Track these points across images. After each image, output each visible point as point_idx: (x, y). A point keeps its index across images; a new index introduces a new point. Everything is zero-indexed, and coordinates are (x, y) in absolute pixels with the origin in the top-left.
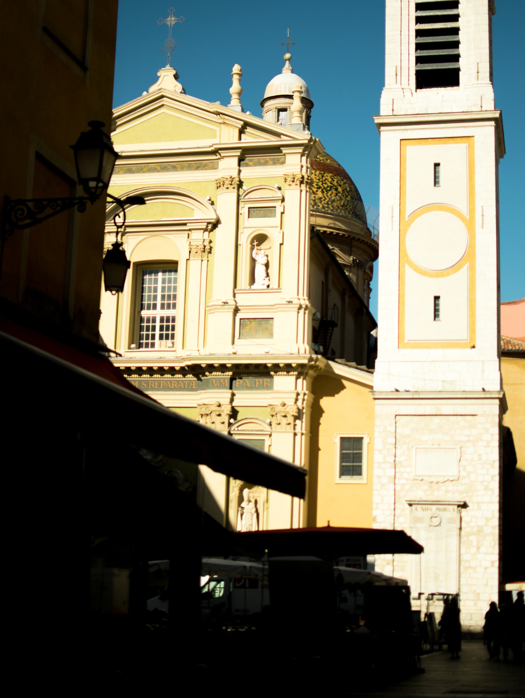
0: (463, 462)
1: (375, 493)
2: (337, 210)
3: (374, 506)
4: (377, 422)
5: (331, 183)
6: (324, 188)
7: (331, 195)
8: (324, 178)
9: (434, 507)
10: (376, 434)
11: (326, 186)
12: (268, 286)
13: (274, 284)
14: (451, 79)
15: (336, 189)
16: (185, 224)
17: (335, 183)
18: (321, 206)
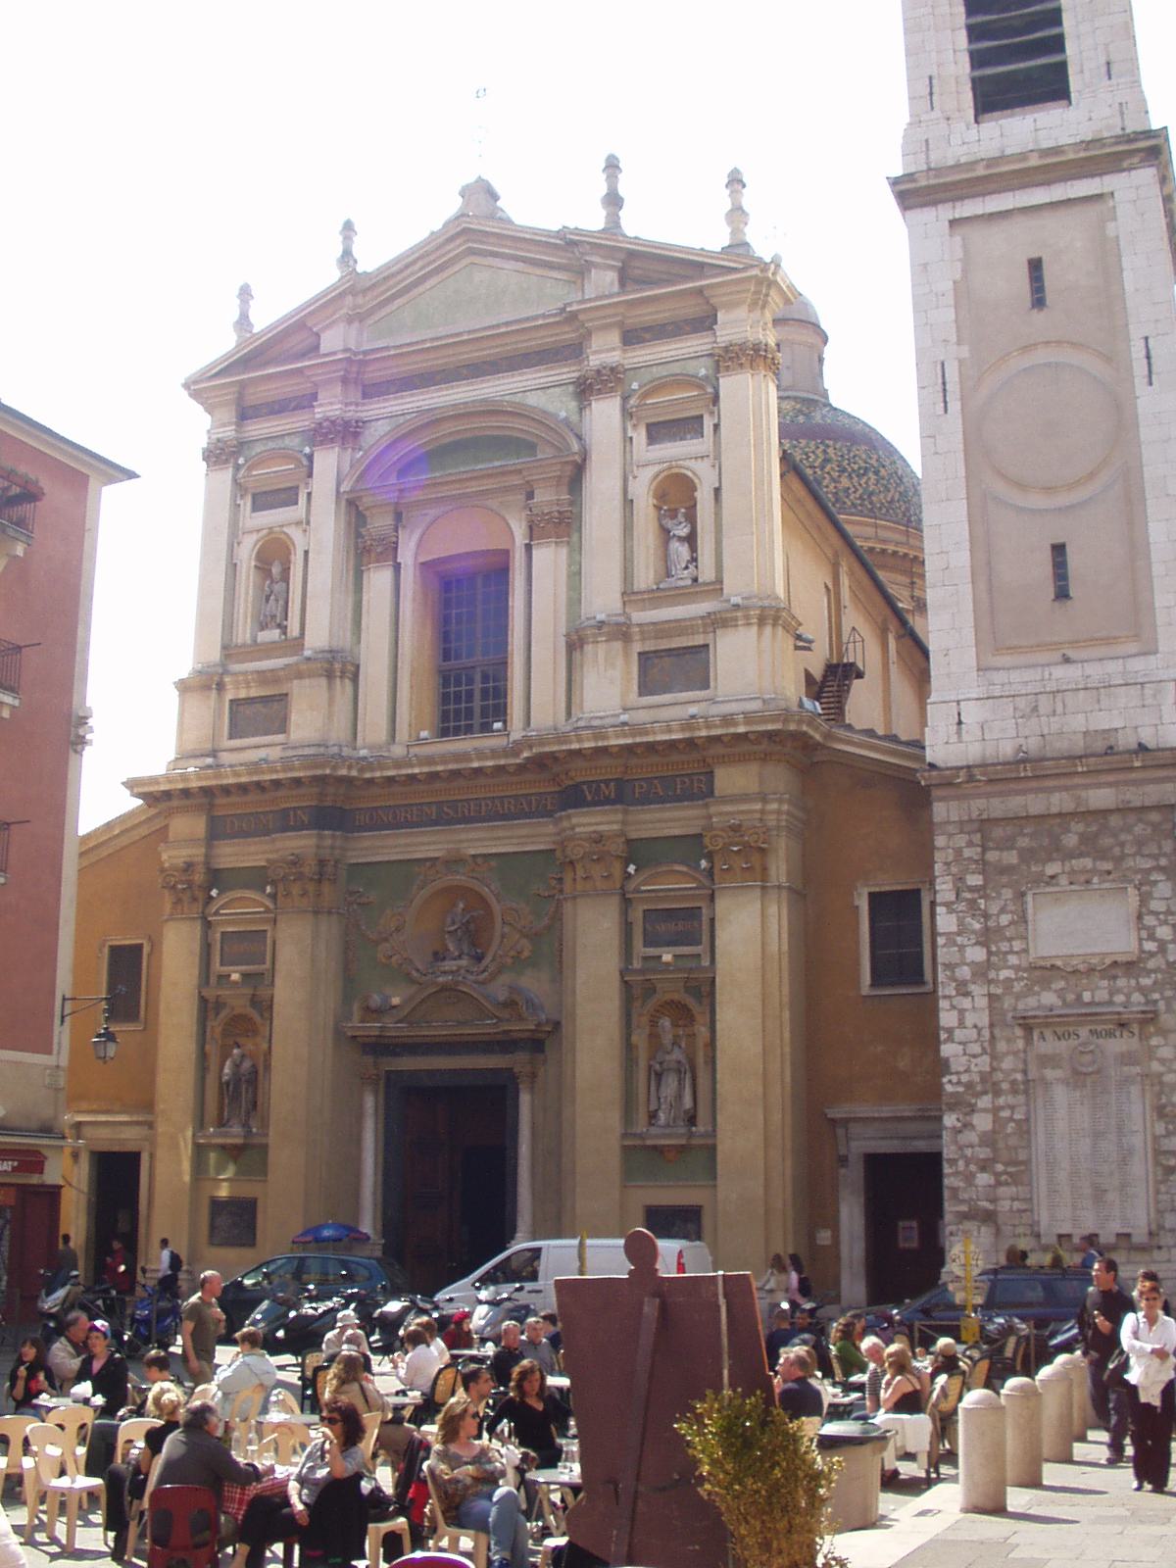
0: (1149, 920)
1: (943, 1004)
2: (880, 508)
3: (943, 1036)
4: (940, 841)
5: (866, 462)
6: (853, 470)
7: (866, 483)
8: (852, 455)
9: (1084, 1032)
10: (938, 868)
11: (856, 467)
12: (695, 580)
13: (707, 574)
14: (1053, 87)
15: (876, 473)
16: (520, 471)
17: (873, 462)
18: (849, 503)
